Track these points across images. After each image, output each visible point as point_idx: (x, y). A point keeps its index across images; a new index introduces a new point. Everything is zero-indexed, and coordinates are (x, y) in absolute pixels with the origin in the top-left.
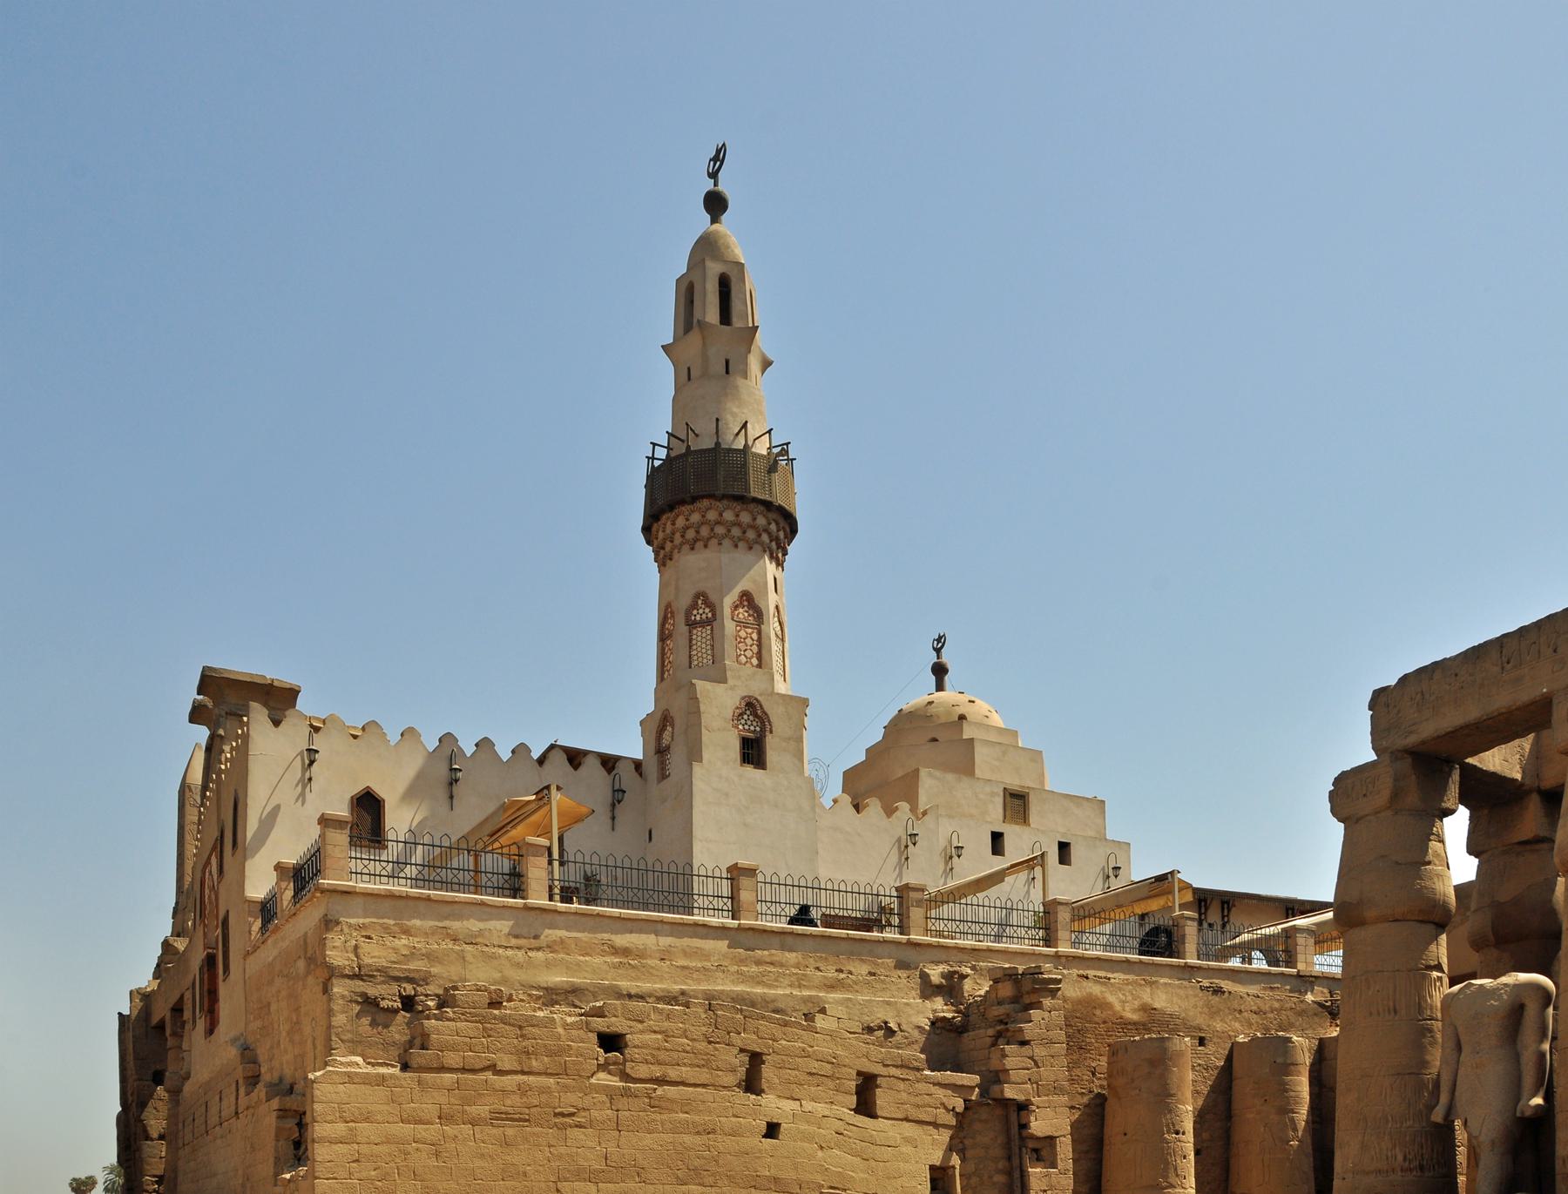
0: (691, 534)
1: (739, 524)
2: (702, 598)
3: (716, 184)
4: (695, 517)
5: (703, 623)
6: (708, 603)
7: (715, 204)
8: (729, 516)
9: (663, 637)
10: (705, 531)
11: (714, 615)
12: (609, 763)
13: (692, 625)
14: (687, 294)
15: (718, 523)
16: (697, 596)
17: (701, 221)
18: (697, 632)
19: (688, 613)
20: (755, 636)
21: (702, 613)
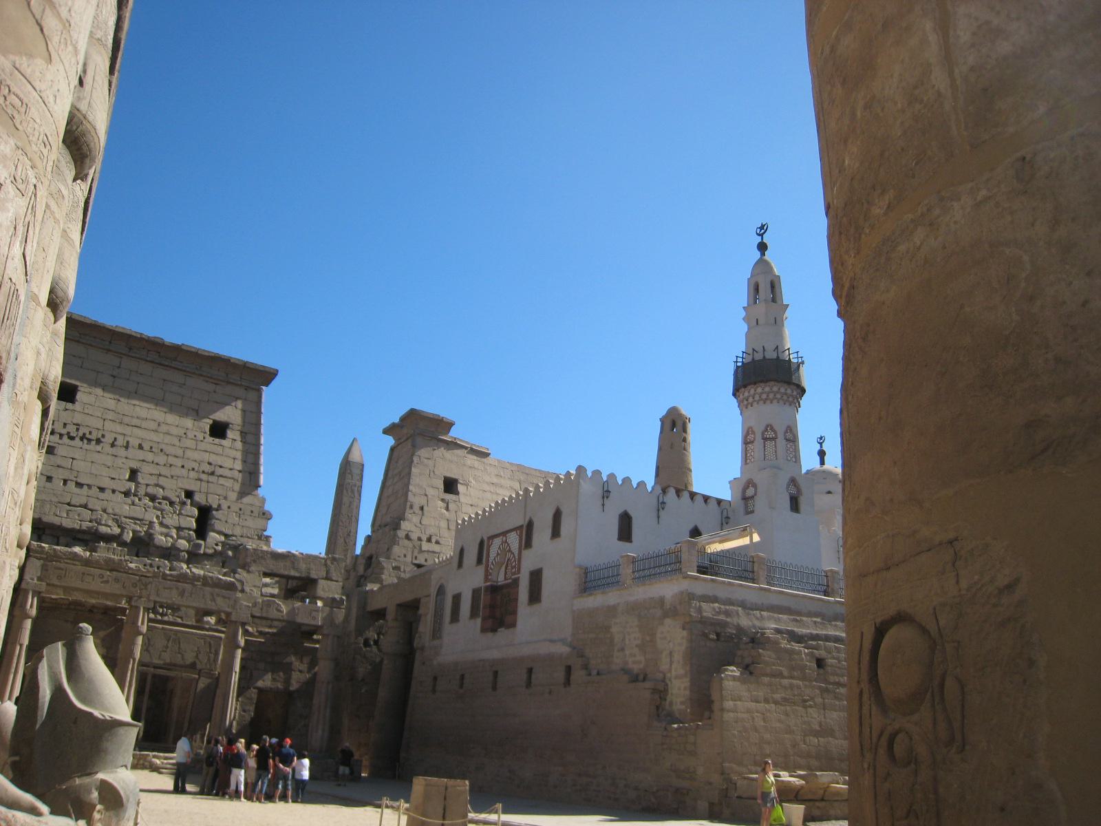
0: (764, 396)
1: (786, 394)
2: (769, 427)
3: (762, 239)
4: (767, 389)
6: (772, 429)
7: (762, 247)
8: (782, 390)
9: (746, 442)
10: (771, 396)
11: (776, 435)
12: (719, 502)
13: (765, 439)
14: (756, 289)
15: (777, 392)
16: (767, 426)
17: (758, 255)
18: (768, 443)
19: (763, 434)
20: (793, 447)
21: (770, 434)
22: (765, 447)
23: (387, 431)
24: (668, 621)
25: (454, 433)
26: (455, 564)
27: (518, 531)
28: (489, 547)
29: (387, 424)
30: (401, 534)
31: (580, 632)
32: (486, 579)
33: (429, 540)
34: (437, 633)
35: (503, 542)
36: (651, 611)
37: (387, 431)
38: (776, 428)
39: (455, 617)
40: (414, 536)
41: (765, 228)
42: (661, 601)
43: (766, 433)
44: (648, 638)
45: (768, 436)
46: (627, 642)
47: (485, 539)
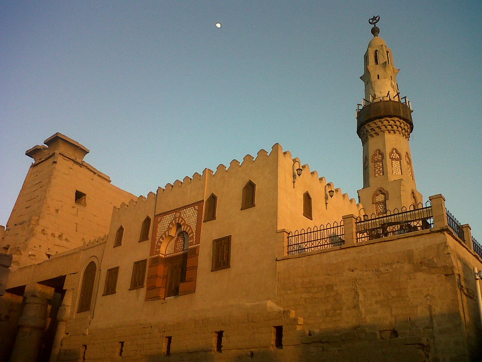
5: (396, 159)
13: (392, 159)
22: (392, 164)
23: (31, 153)
24: (421, 276)
25: (87, 159)
26: (112, 240)
27: (196, 207)
28: (156, 223)
29: (30, 146)
30: (38, 229)
31: (289, 292)
32: (152, 253)
33: (60, 236)
34: (85, 305)
35: (175, 218)
36: (394, 266)
37: (31, 153)
38: (399, 151)
39: (110, 289)
40: (49, 232)
41: (377, 19)
42: (409, 256)
43: (392, 155)
44: (394, 294)
45: (394, 157)
46: (361, 298)
47: (152, 217)
